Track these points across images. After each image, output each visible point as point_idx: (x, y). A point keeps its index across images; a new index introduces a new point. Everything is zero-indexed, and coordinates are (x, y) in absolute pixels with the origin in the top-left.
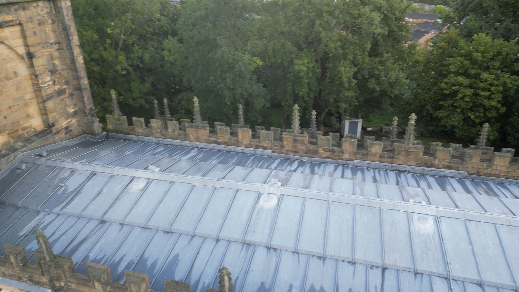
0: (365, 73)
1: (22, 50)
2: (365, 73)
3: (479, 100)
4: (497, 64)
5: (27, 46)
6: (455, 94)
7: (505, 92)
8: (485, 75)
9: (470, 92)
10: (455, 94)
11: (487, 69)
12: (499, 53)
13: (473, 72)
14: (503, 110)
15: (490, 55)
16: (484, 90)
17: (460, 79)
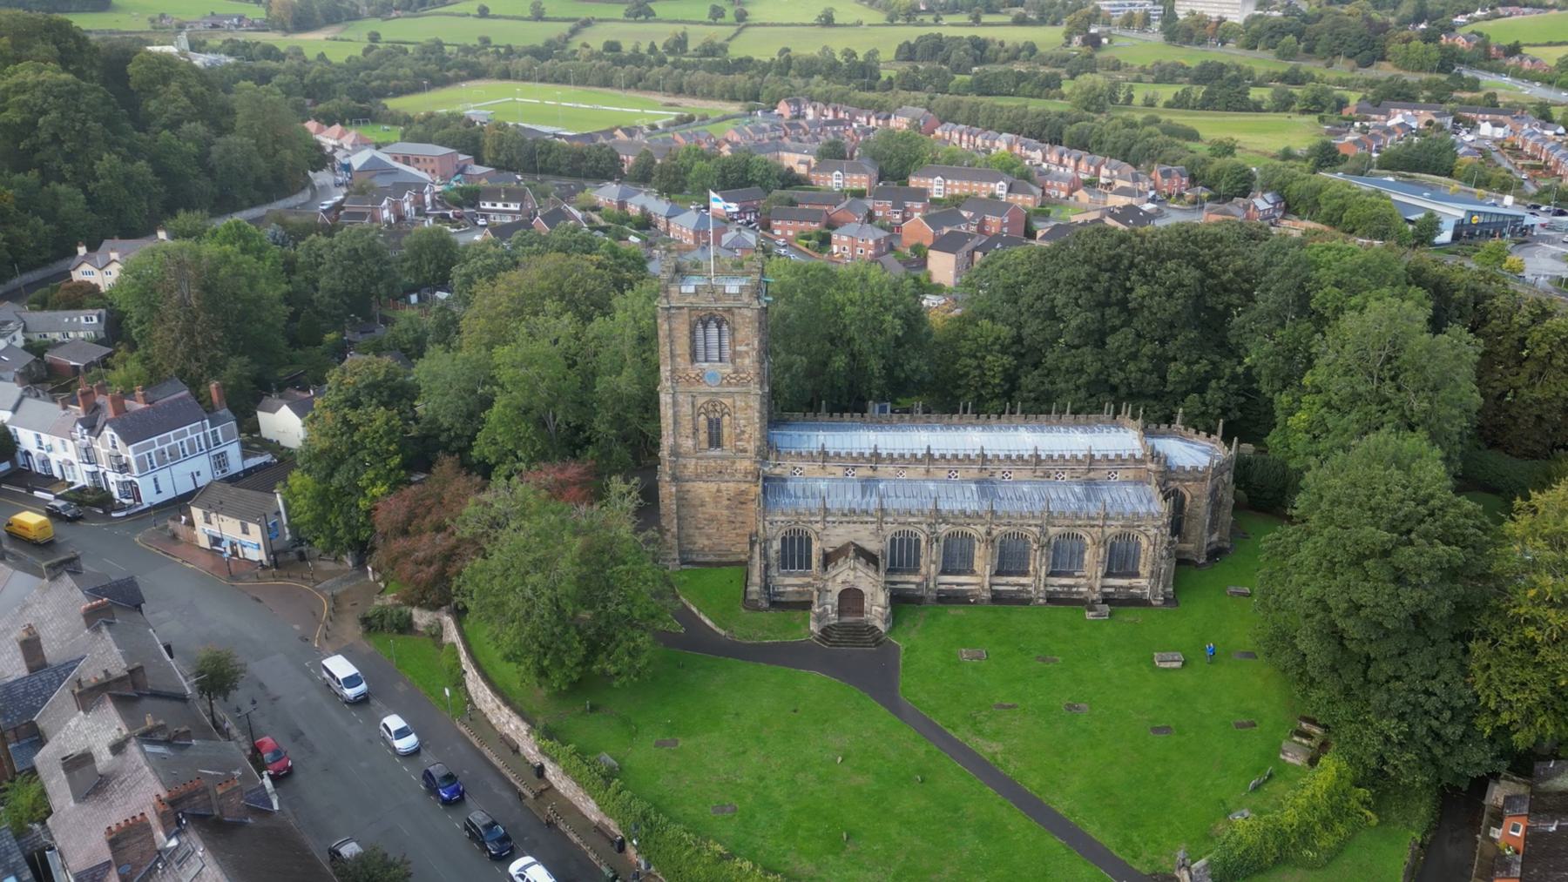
0: (891, 363)
2: (891, 363)
3: (986, 379)
4: (997, 347)
6: (967, 374)
7: (1005, 370)
8: (989, 358)
9: (977, 372)
10: (967, 374)
11: (990, 352)
12: (998, 338)
13: (979, 354)
14: (1007, 387)
15: (991, 339)
16: (990, 370)
17: (968, 361)
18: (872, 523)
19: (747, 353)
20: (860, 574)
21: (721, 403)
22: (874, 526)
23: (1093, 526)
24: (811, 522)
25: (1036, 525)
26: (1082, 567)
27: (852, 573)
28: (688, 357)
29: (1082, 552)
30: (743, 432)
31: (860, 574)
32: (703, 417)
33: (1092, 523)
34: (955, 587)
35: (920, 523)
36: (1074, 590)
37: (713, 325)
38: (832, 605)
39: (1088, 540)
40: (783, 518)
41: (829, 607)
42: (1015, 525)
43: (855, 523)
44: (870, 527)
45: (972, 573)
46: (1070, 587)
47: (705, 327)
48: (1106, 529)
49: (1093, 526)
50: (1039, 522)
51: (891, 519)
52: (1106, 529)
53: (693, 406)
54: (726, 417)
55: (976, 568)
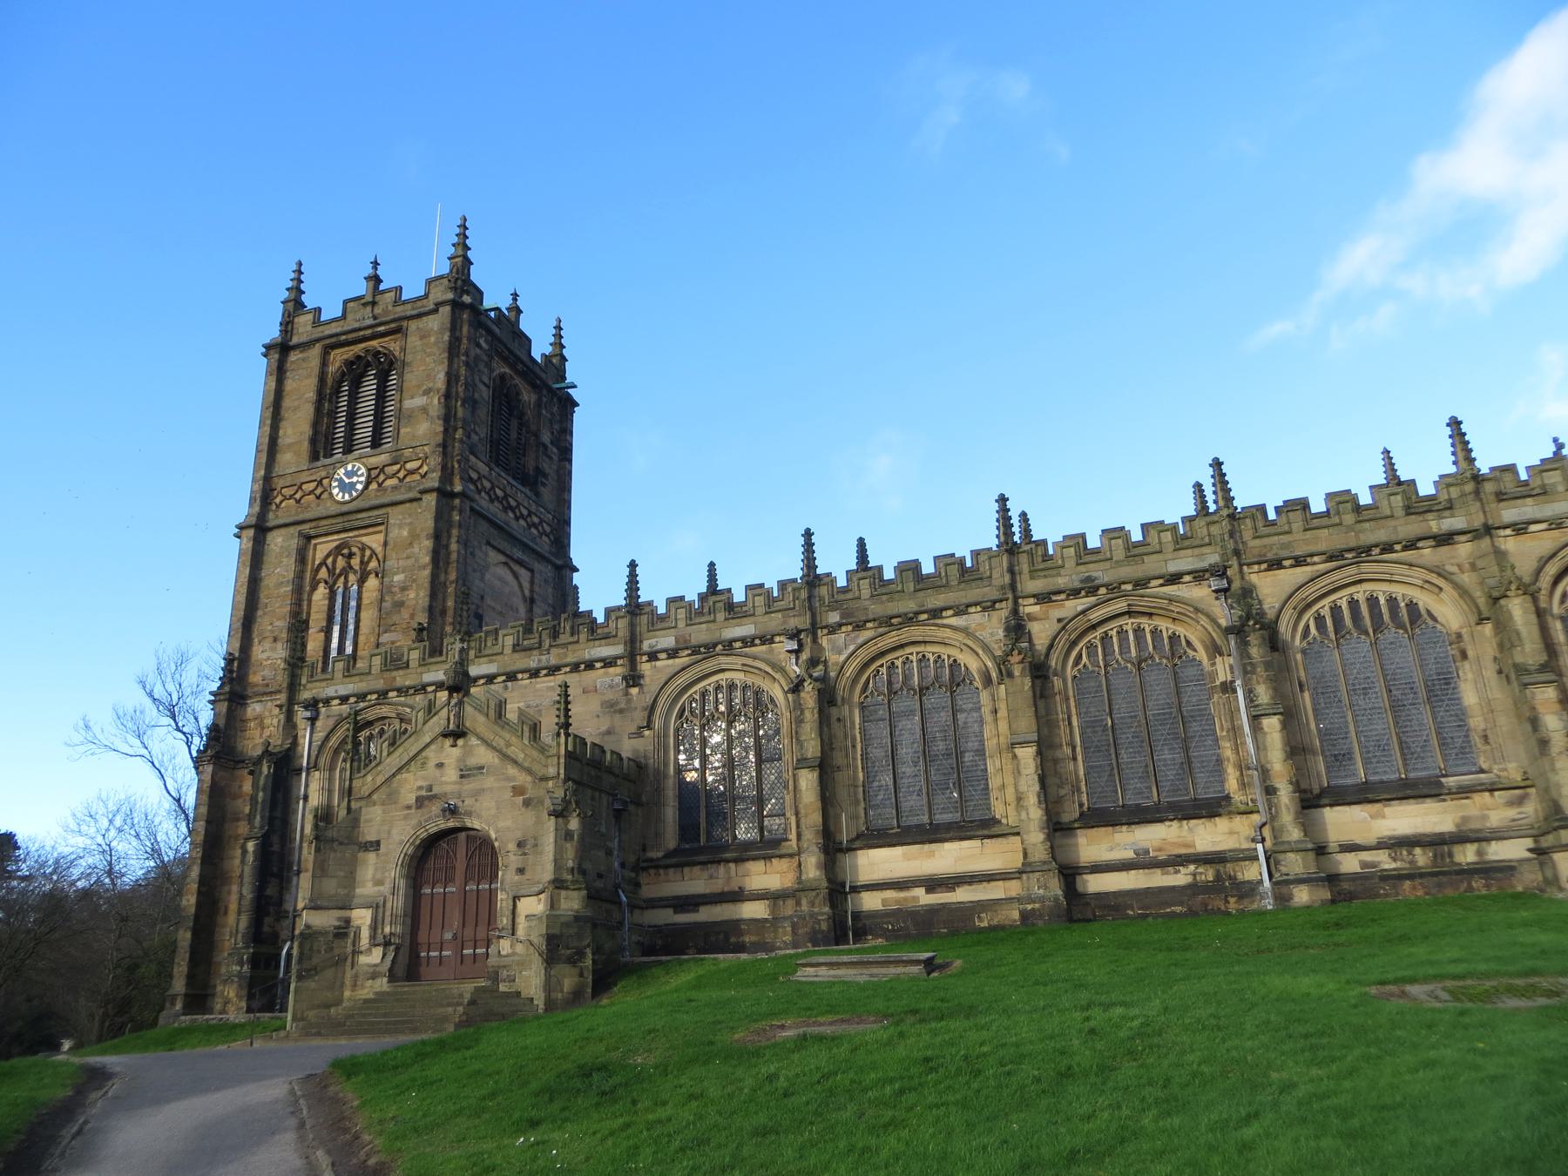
1: (527, 593)
5: (532, 591)
18: (609, 663)
19: (424, 409)
20: (483, 756)
21: (363, 548)
22: (617, 672)
23: (1445, 539)
24: (422, 688)
25: (1199, 576)
26: (1465, 751)
27: (451, 754)
28: (306, 445)
29: (1441, 688)
30: (399, 605)
31: (483, 756)
32: (321, 592)
33: (1436, 525)
34: (922, 897)
35: (767, 639)
36: (1467, 855)
37: (370, 386)
38: (377, 907)
39: (1449, 613)
40: (343, 690)
41: (362, 918)
42: (1114, 588)
43: (553, 670)
44: (600, 677)
45: (984, 827)
46: (1438, 843)
47: (356, 384)
48: (1509, 543)
49: (1445, 539)
50: (1212, 558)
51: (667, 641)
52: (1509, 543)
53: (302, 558)
54: (372, 582)
55: (998, 810)
